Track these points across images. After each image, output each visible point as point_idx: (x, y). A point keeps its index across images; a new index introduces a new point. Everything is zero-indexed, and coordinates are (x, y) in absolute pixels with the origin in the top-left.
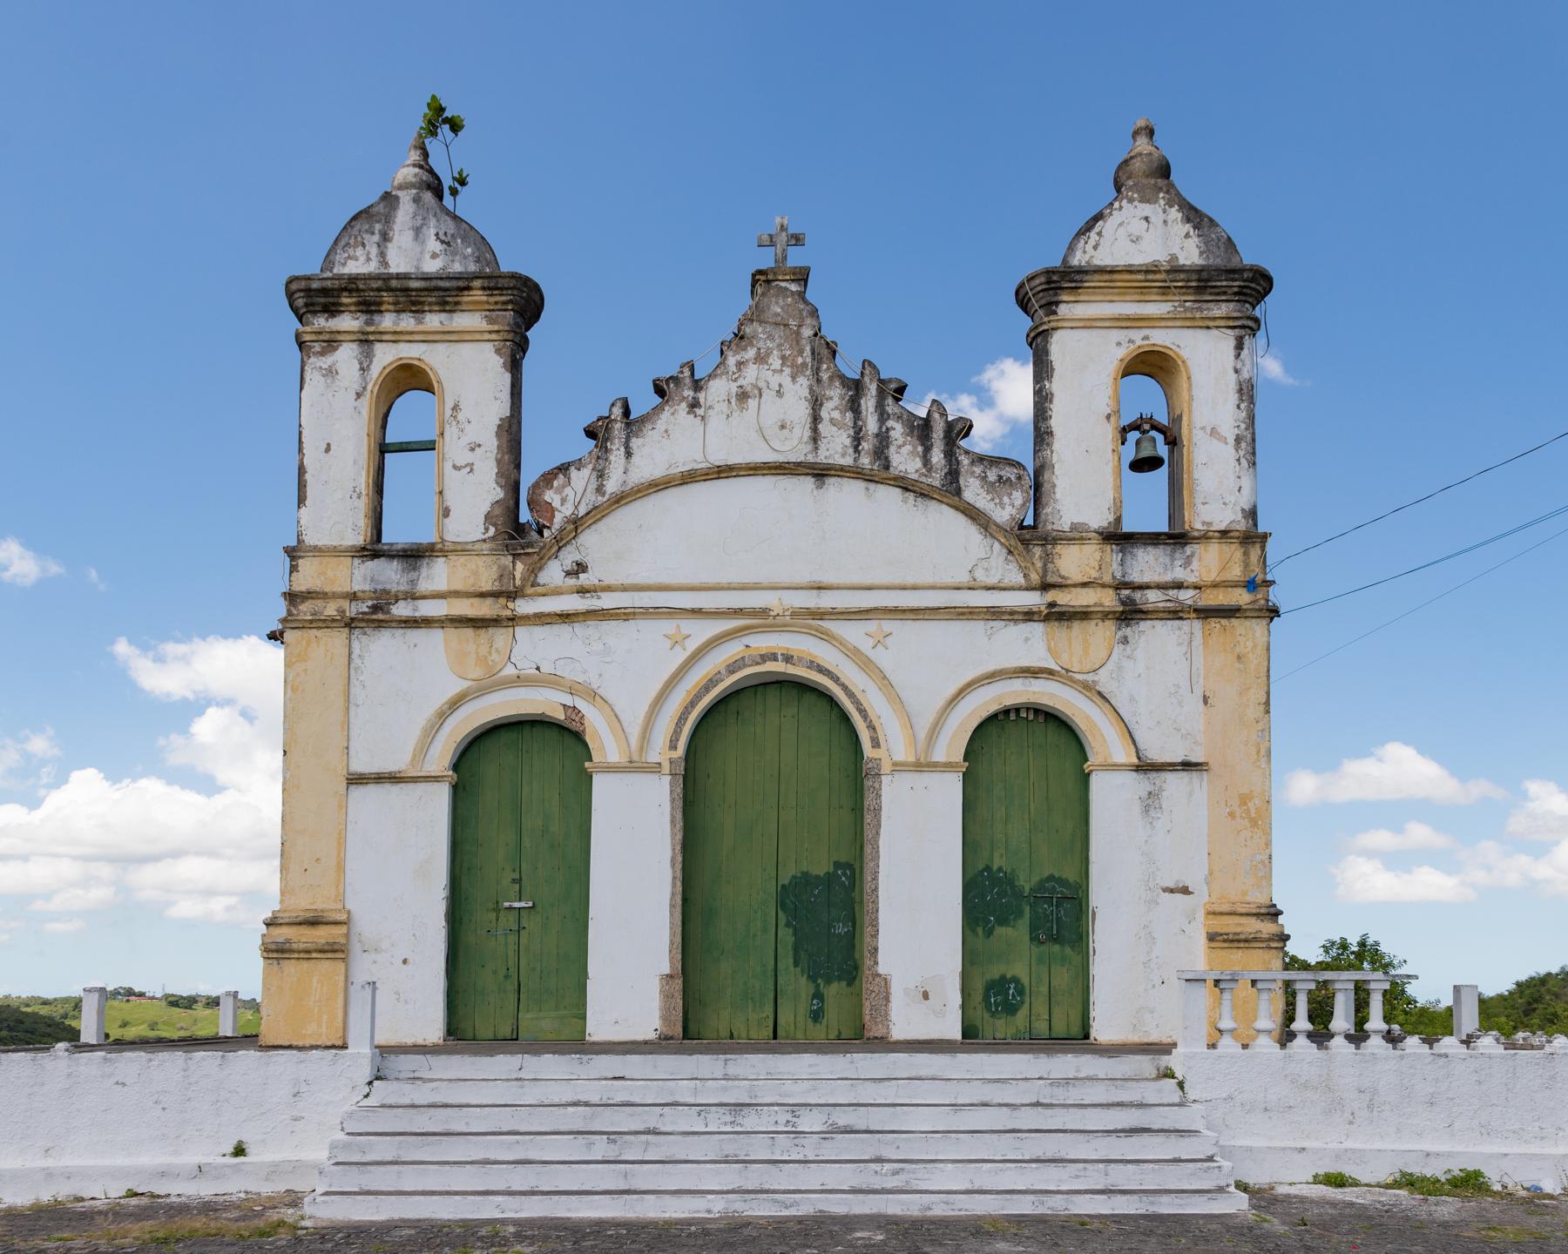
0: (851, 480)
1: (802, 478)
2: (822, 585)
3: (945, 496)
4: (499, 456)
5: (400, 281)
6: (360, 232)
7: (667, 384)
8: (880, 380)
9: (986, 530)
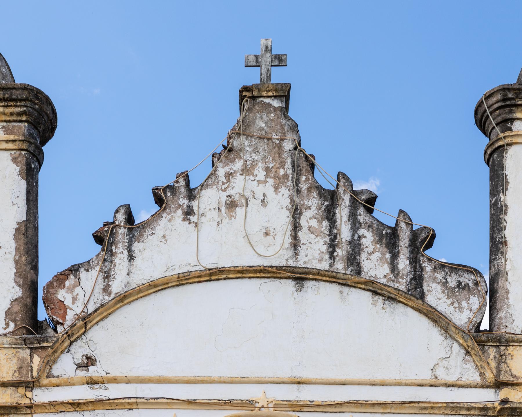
0: (327, 284)
1: (284, 281)
2: (302, 380)
3: (410, 299)
4: (17, 257)
7: (165, 193)
8: (352, 191)
9: (446, 332)
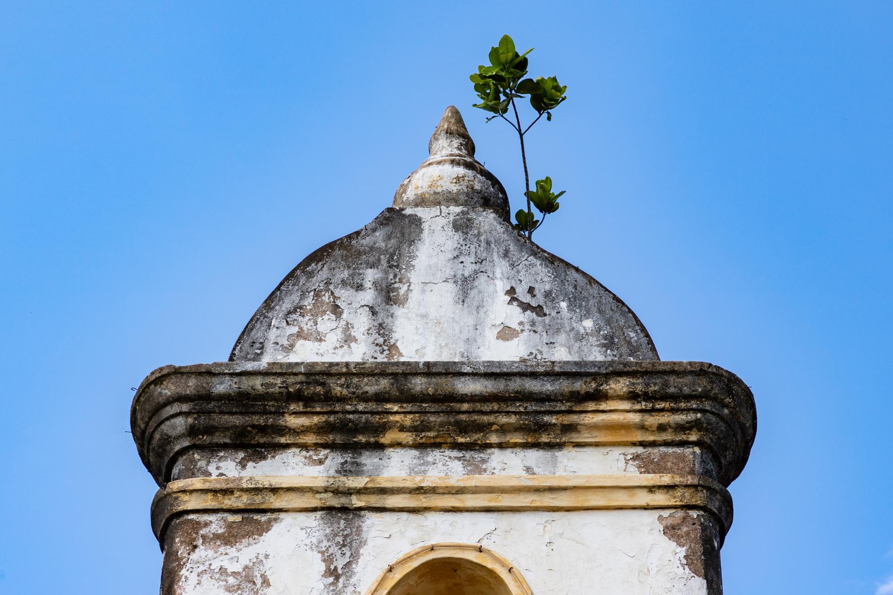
5: (434, 380)
6: (328, 283)
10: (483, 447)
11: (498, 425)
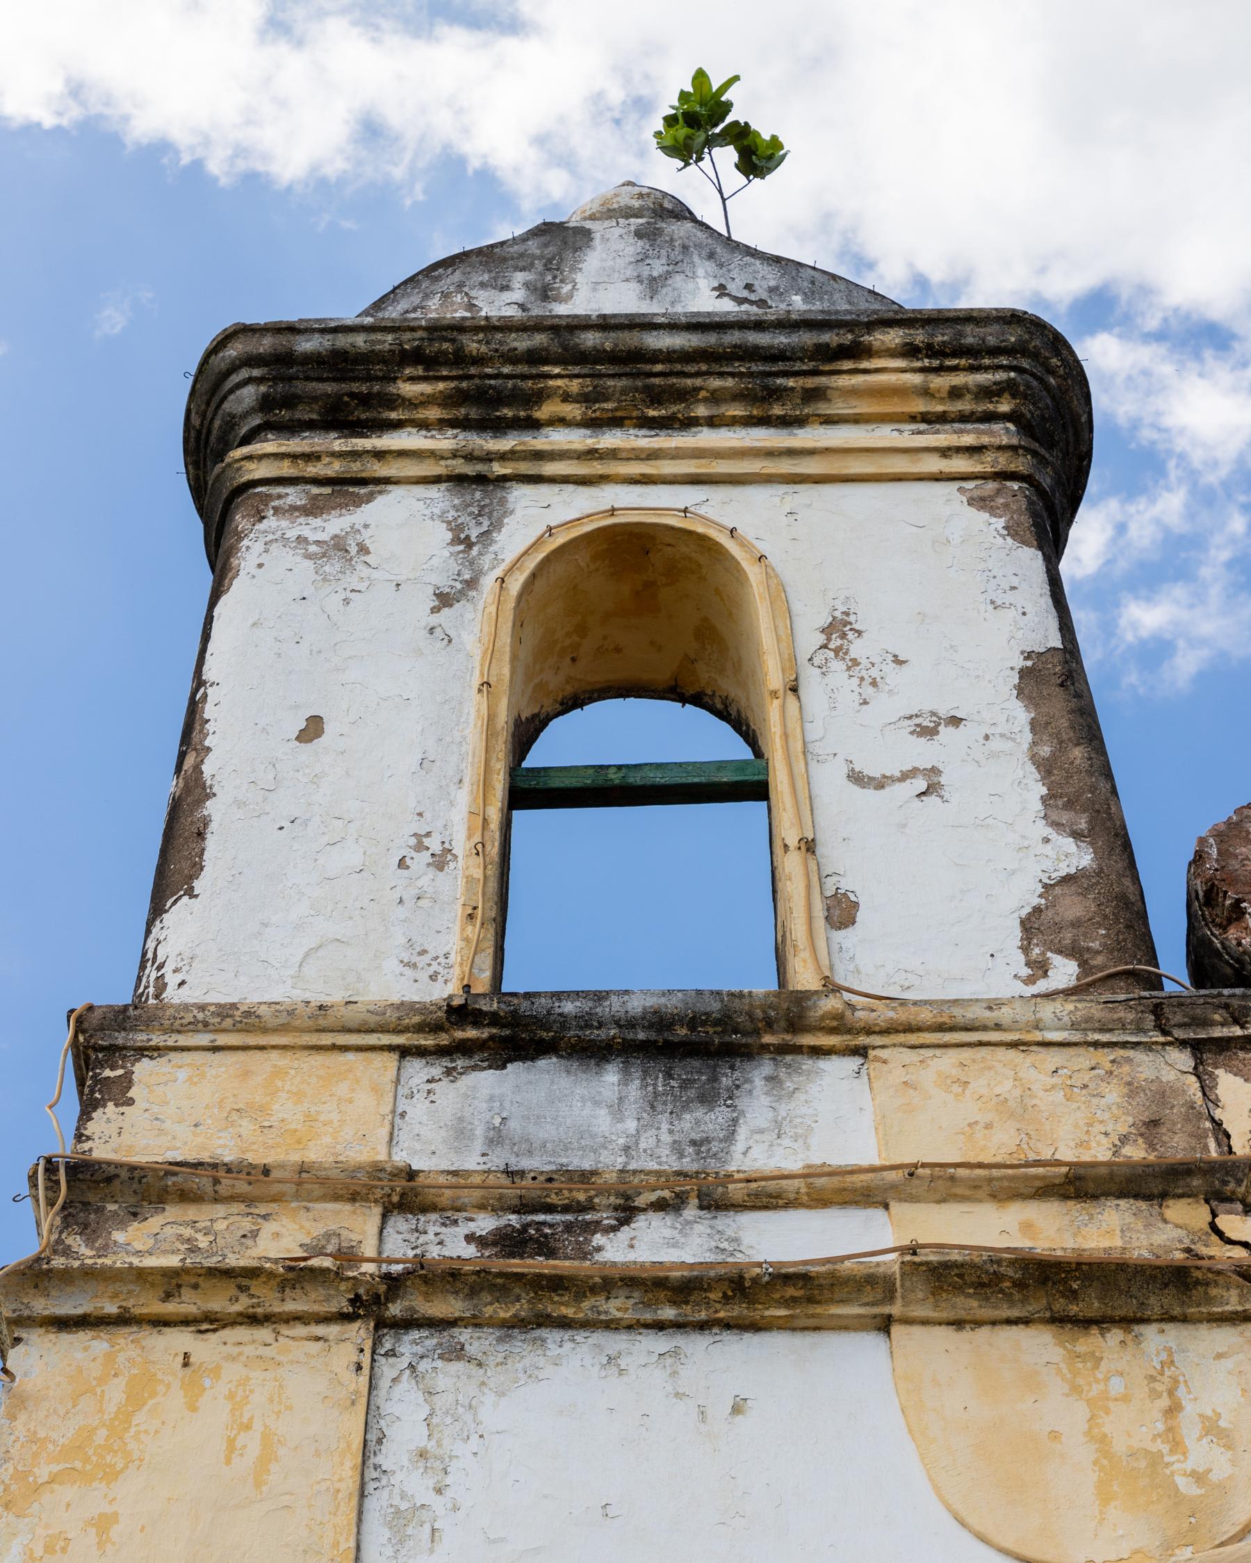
10: (685, 424)
11: (708, 391)
